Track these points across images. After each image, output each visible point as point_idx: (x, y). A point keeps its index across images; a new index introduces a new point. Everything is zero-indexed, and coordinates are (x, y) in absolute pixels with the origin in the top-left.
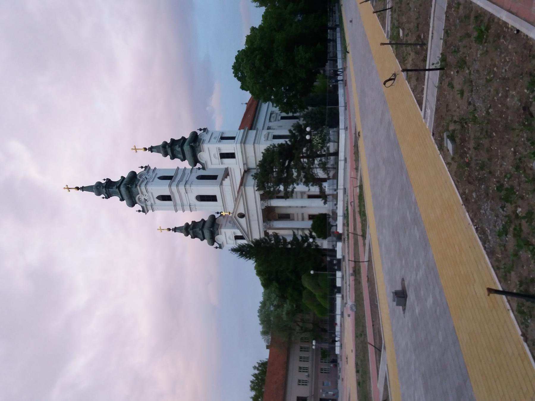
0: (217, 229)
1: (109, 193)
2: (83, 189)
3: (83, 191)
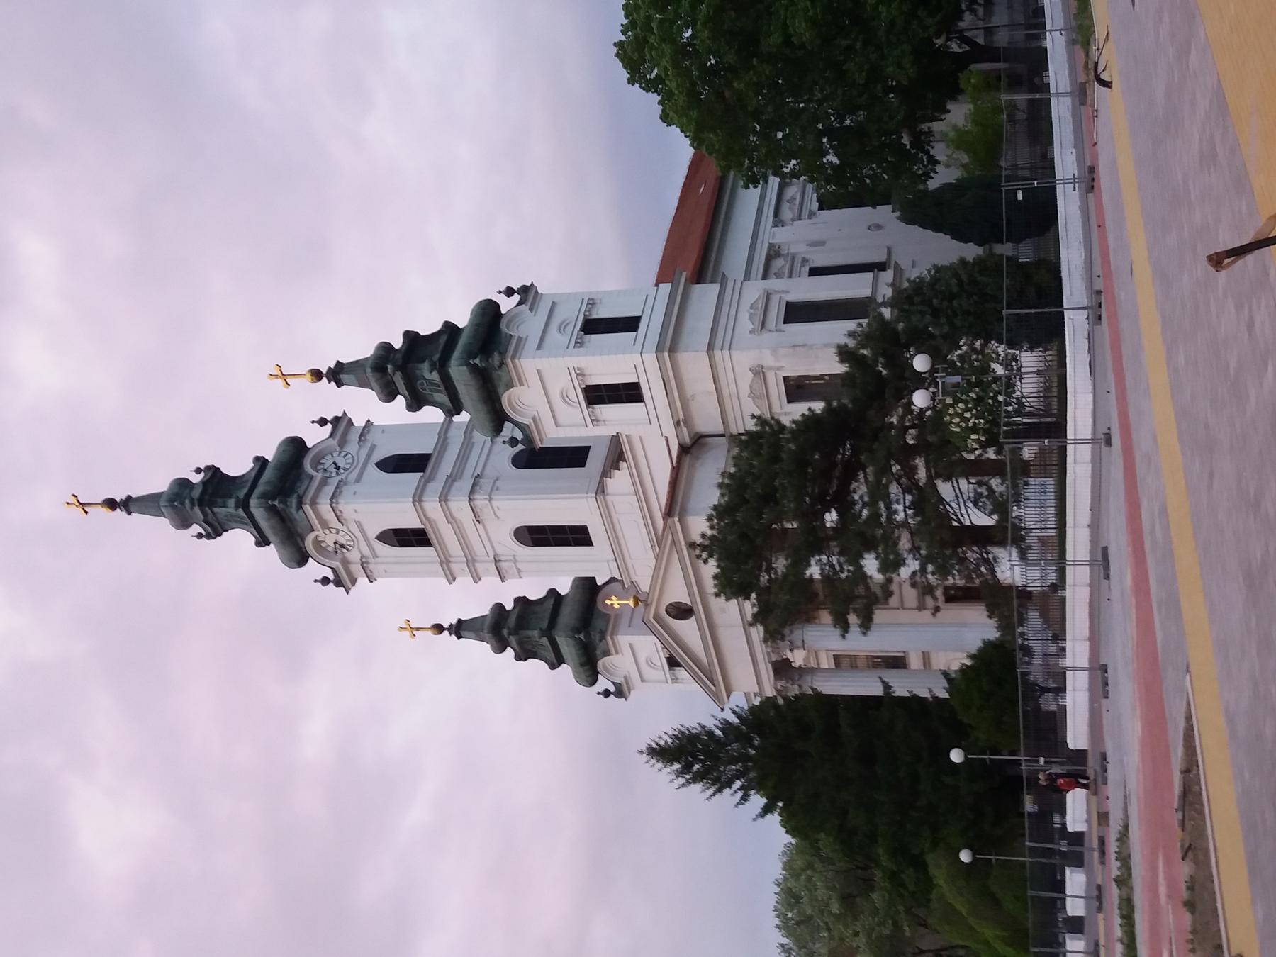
0: (603, 638)
2: (128, 505)
3: (129, 513)
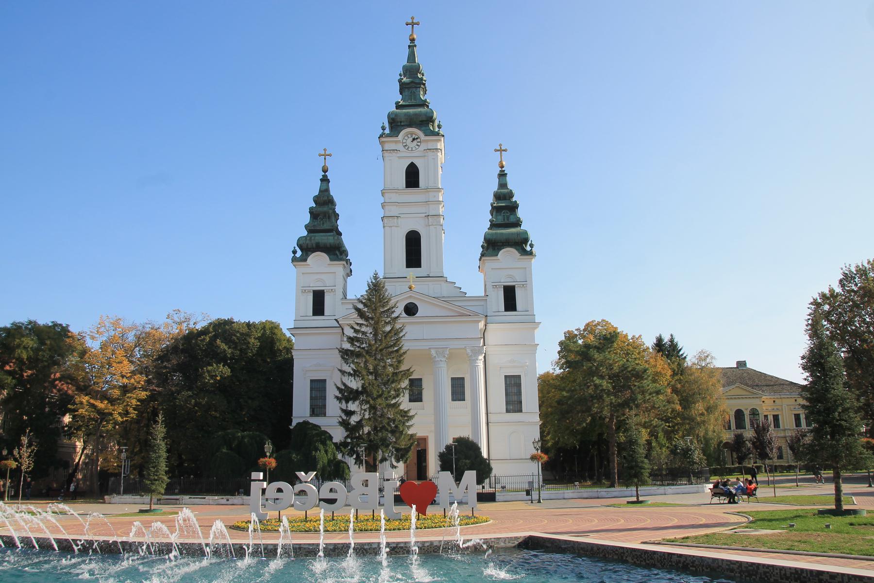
1: (410, 88)
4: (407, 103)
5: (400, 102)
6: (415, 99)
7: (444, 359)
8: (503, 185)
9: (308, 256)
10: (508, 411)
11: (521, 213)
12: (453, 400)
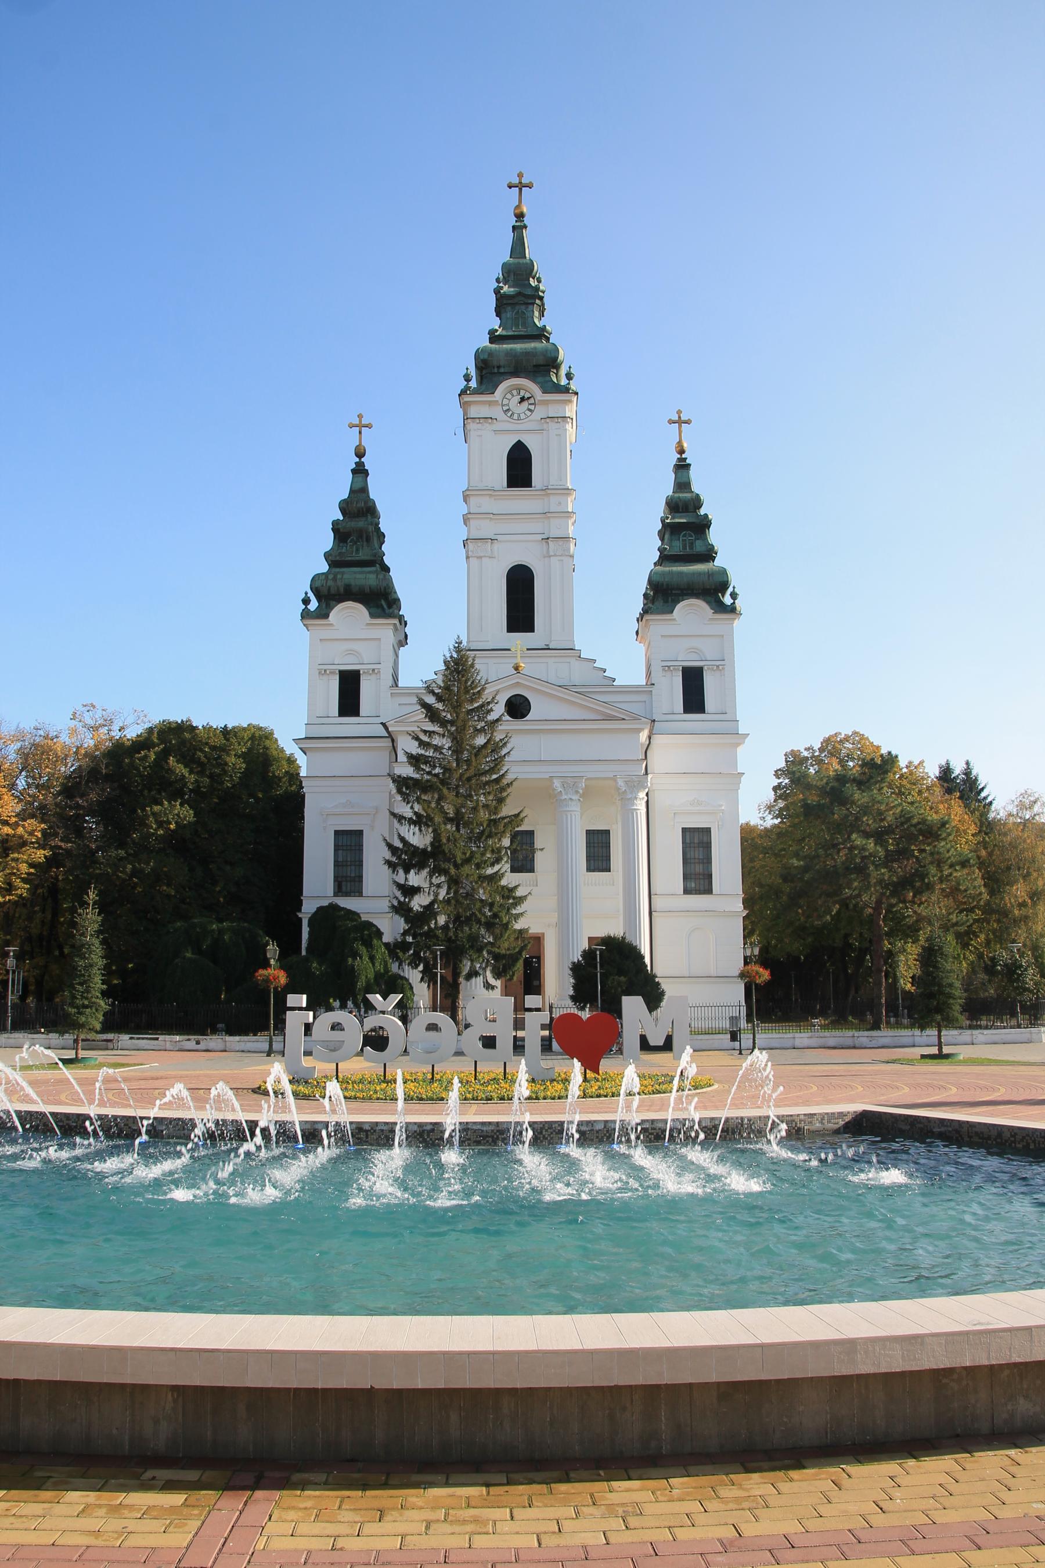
4: (510, 333)
5: (497, 331)
6: (524, 325)
7: (575, 797)
8: (683, 484)
9: (330, 608)
10: (687, 891)
11: (714, 536)
12: (589, 870)
